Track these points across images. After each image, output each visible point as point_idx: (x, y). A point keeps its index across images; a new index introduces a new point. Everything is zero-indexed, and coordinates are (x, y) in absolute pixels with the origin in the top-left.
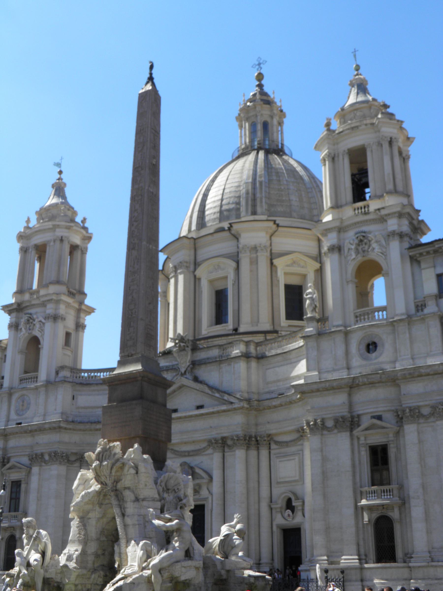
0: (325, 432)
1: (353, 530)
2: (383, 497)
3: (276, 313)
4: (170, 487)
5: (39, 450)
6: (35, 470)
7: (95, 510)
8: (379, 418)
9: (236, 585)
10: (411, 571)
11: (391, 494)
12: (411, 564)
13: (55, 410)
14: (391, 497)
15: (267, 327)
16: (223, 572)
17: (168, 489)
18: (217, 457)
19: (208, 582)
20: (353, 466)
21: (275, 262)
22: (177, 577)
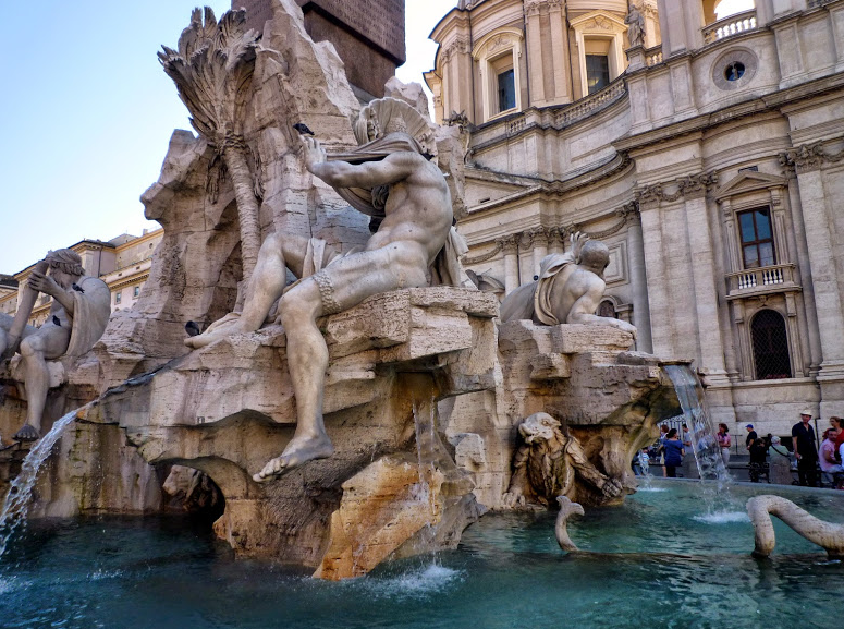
0: (665, 203)
1: (717, 334)
2: (766, 283)
3: (576, 87)
8: (754, 168)
9: (599, 392)
10: (819, 388)
11: (780, 276)
12: (818, 379)
14: (781, 281)
15: (567, 101)
16: (557, 360)
18: (510, 259)
19: (513, 388)
20: (713, 244)
21: (572, 23)
22: (395, 345)
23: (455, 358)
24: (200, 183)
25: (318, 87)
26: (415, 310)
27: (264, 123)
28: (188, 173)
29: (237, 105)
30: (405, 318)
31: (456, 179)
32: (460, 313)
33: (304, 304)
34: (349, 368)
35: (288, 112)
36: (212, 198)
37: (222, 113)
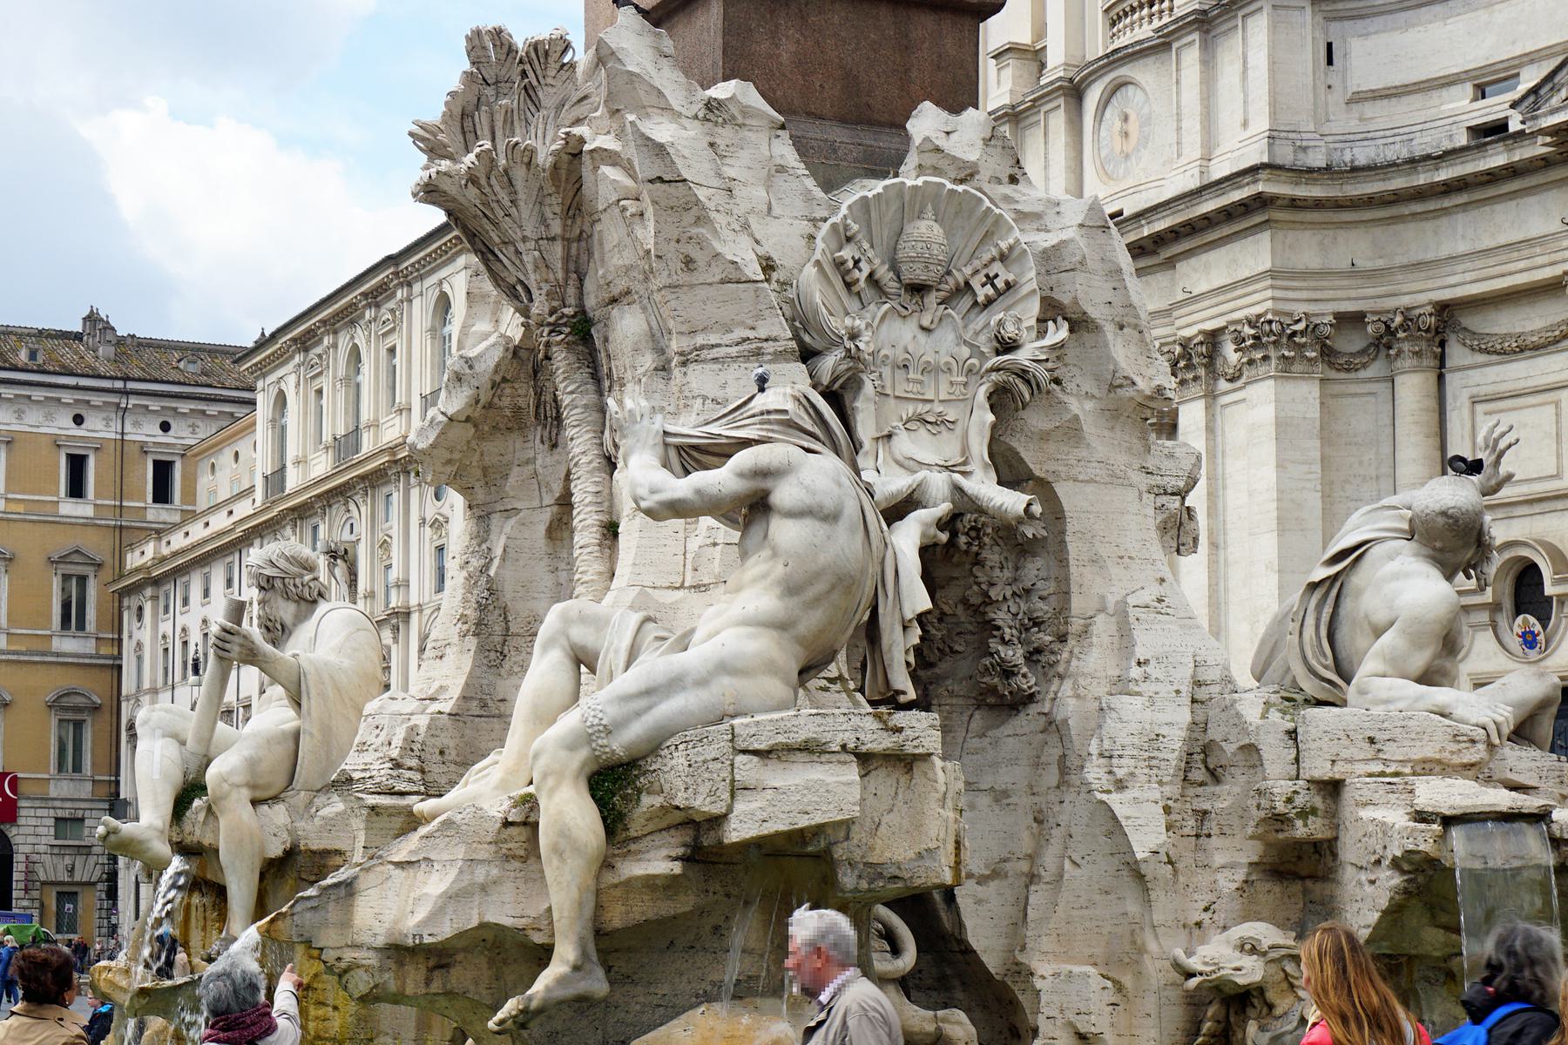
4: (916, 273)
5: (1194, 324)
6: (1191, 416)
7: (533, 460)
13: (1245, 124)
17: (918, 289)
19: (1219, 859)
22: (717, 821)
23: (842, 834)
24: (521, 402)
25: (694, 231)
26: (740, 758)
27: (616, 291)
28: (494, 385)
29: (567, 241)
30: (725, 774)
31: (1110, 330)
32: (834, 758)
33: (563, 754)
34: (647, 856)
35: (646, 279)
36: (546, 434)
37: (537, 268)
